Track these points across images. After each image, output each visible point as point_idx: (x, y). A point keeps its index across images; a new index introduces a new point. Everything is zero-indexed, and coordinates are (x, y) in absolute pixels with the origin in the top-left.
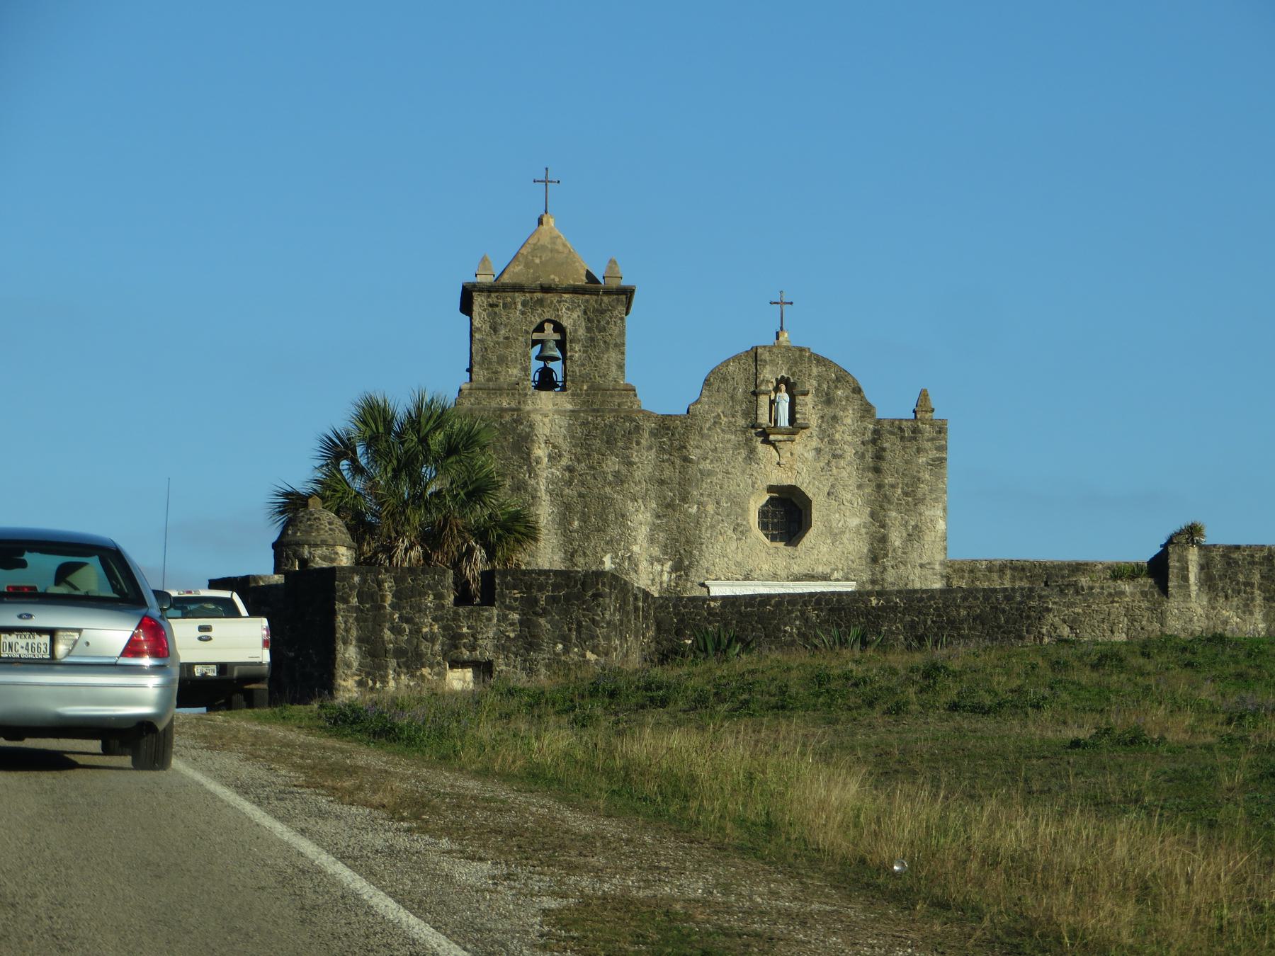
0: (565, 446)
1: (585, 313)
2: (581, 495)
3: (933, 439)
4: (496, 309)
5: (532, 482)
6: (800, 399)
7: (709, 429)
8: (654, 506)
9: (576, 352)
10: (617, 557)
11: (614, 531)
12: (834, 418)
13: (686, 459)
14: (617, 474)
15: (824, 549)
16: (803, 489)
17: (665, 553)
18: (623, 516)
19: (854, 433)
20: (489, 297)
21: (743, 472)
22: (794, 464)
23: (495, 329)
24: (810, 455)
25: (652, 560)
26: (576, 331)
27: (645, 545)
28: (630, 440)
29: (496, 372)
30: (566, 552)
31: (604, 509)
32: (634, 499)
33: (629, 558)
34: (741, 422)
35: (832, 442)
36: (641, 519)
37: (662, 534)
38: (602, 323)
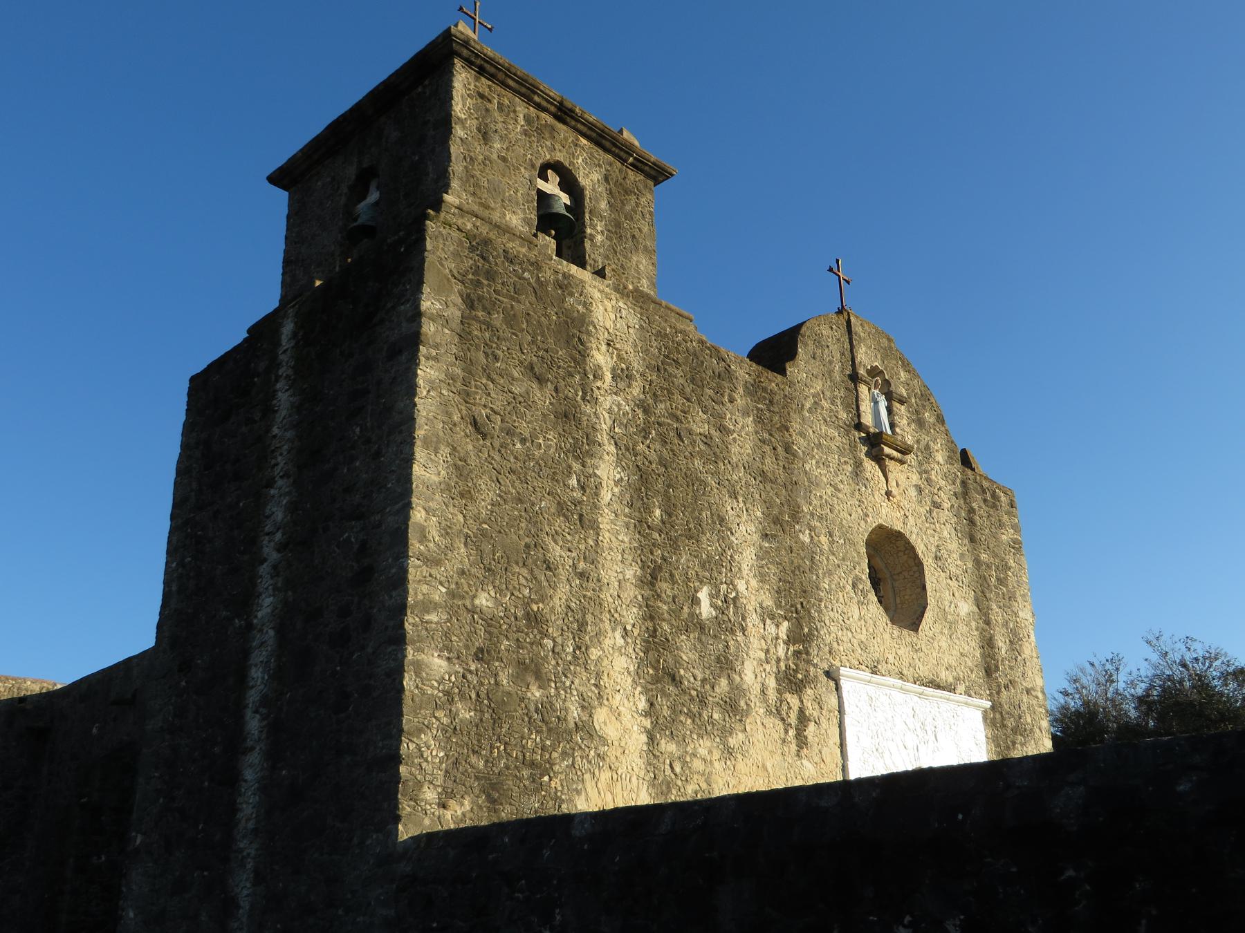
0: (637, 365)
1: (606, 179)
2: (662, 463)
3: (1008, 513)
4: (489, 106)
5: (588, 409)
6: (896, 405)
7: (810, 411)
8: (759, 514)
9: (597, 232)
10: (717, 596)
11: (710, 545)
12: (927, 447)
13: (788, 449)
14: (707, 440)
15: (944, 645)
16: (913, 539)
17: (779, 606)
18: (722, 520)
19: (946, 477)
20: (477, 79)
21: (853, 494)
22: (903, 499)
23: (485, 135)
24: (913, 493)
25: (767, 615)
26: (597, 201)
27: (754, 583)
28: (719, 391)
29: (487, 207)
30: (643, 567)
31: (695, 498)
32: (734, 495)
33: (734, 599)
34: (843, 415)
35: (928, 480)
36: (746, 531)
37: (773, 569)
38: (628, 208)
